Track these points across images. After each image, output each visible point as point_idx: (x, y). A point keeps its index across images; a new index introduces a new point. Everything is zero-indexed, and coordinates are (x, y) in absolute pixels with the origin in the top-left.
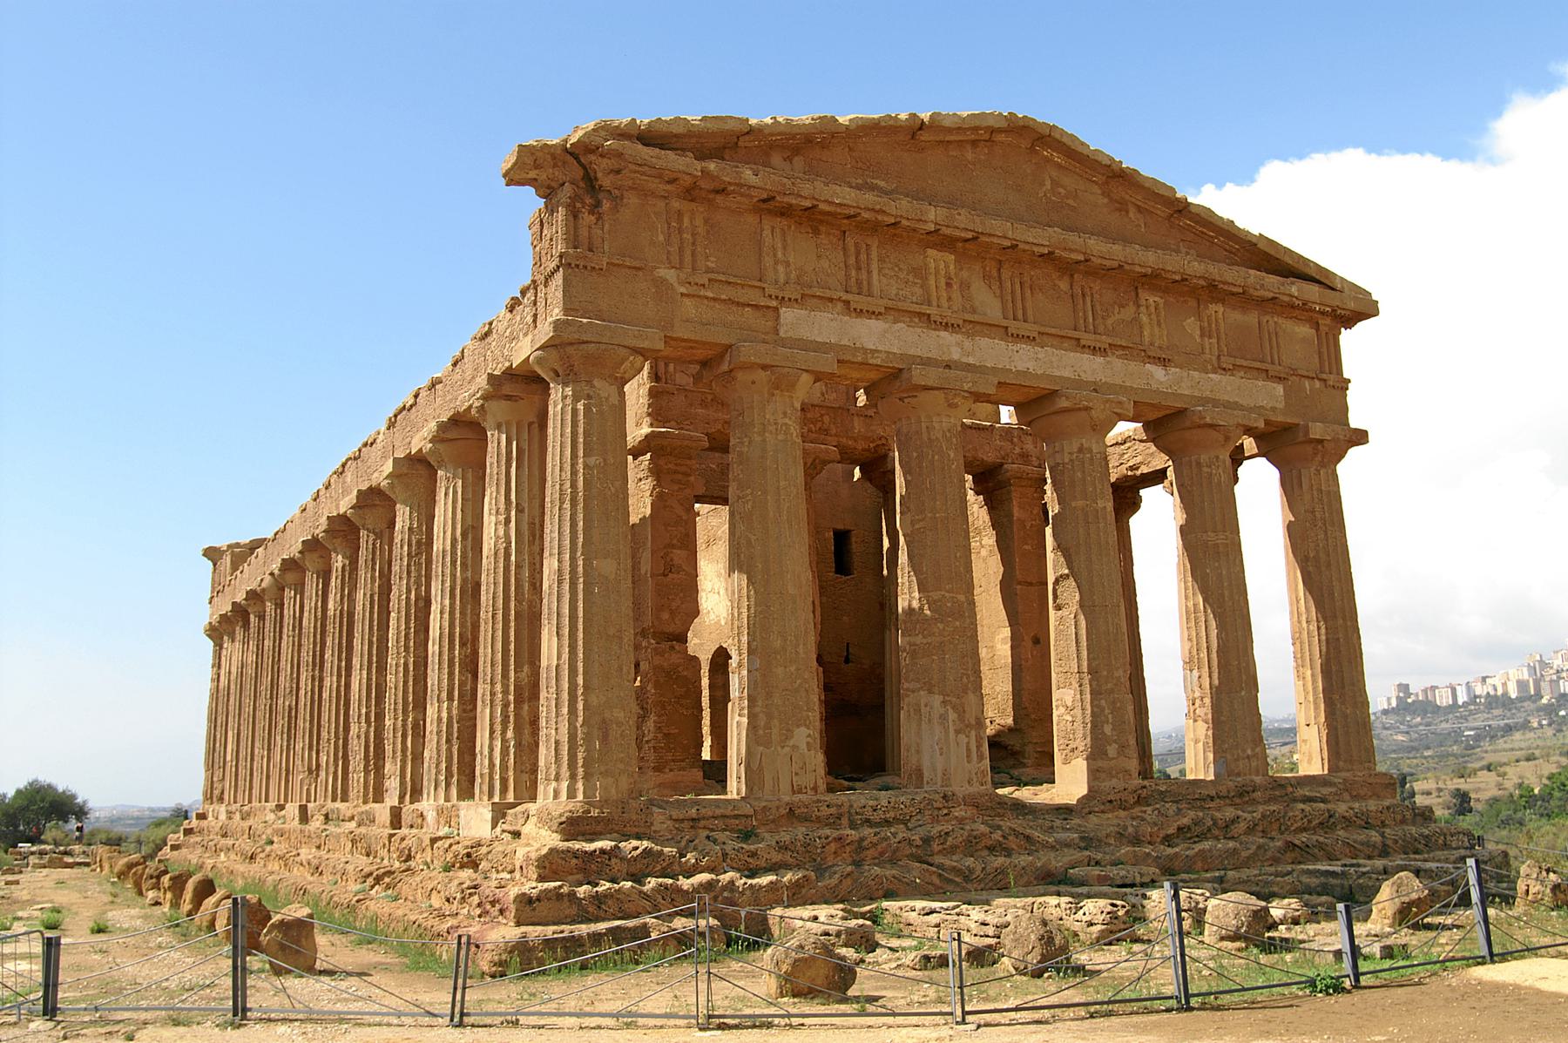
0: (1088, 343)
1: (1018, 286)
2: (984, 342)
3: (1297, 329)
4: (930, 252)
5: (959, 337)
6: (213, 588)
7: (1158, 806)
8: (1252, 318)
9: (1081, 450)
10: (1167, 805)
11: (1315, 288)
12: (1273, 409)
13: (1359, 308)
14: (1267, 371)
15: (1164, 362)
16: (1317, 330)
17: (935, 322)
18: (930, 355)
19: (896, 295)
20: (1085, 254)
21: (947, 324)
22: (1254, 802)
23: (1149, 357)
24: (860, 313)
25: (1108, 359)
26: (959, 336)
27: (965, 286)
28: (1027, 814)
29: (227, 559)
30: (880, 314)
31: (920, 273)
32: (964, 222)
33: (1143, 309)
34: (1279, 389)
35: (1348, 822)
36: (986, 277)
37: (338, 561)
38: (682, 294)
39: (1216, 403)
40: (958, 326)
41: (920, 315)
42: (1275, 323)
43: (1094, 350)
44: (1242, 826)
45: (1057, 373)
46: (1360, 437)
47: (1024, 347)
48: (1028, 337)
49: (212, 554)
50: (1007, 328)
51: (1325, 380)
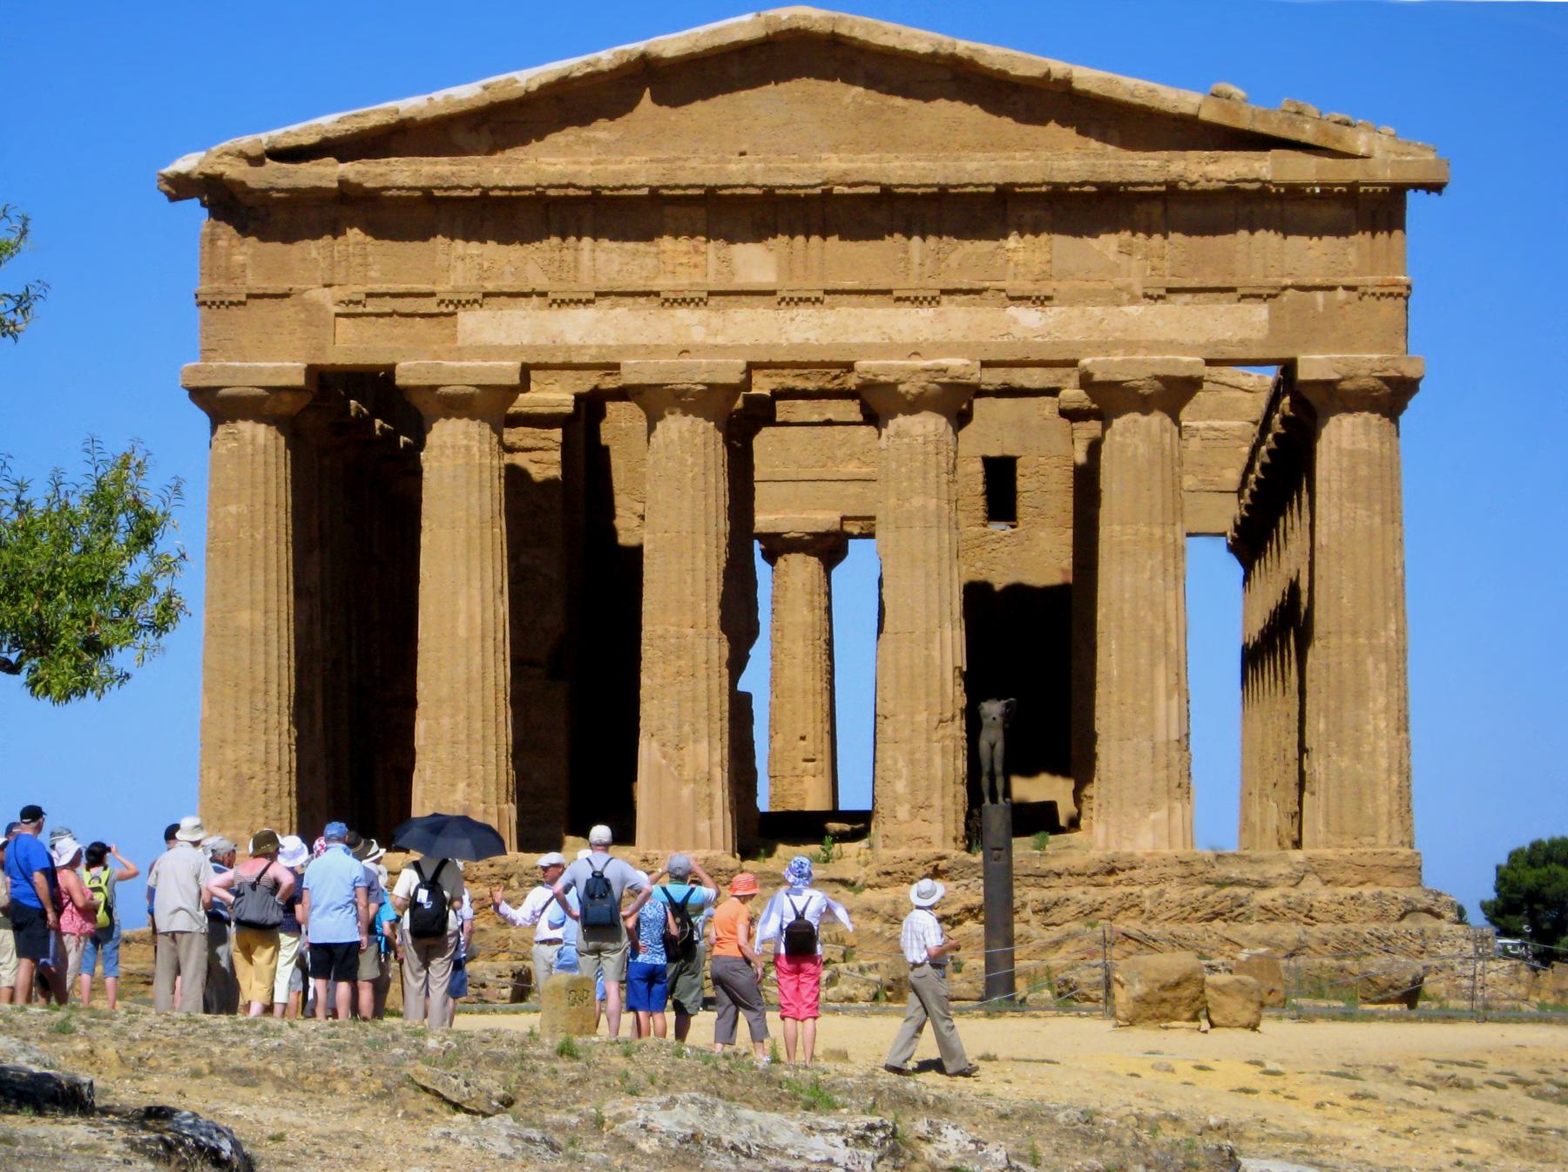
7: (965, 882)
9: (898, 435)
12: (1242, 342)
15: (1043, 301)
17: (667, 300)
19: (620, 271)
22: (1132, 882)
23: (1012, 299)
25: (940, 309)
30: (589, 302)
35: (1270, 914)
38: (338, 315)
39: (1130, 346)
40: (701, 300)
43: (917, 301)
44: (1072, 909)
45: (855, 340)
47: (804, 312)
50: (773, 293)
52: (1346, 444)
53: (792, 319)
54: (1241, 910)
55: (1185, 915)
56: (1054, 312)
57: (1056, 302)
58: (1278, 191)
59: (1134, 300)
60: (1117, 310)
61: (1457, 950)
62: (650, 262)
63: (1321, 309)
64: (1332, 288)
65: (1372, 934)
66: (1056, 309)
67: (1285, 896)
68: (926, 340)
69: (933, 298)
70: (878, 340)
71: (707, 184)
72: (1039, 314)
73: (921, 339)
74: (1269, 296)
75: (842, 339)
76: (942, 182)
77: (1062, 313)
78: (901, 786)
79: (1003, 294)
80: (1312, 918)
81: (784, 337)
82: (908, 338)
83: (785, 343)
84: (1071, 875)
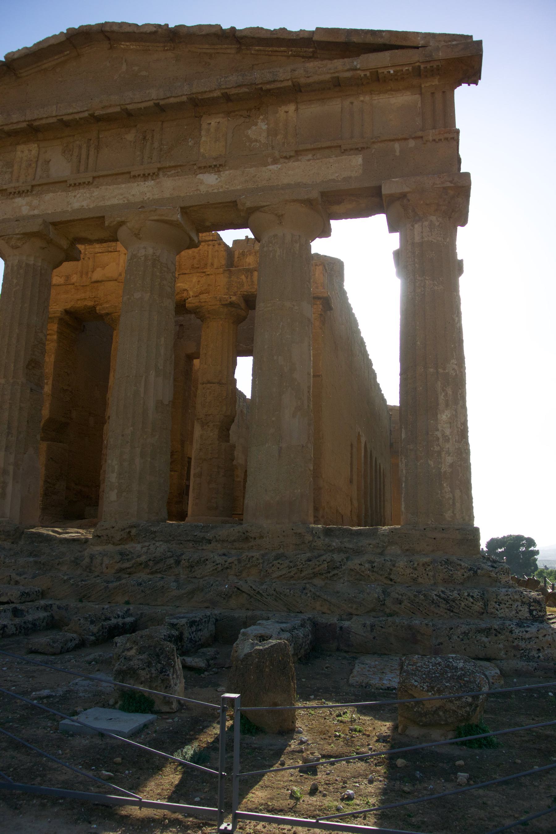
0: (137, 173)
1: (84, 151)
2: (48, 197)
3: (393, 101)
4: (20, 148)
5: (28, 199)
7: (147, 544)
10: (158, 544)
11: (387, 55)
14: (340, 146)
16: (421, 94)
17: (10, 193)
18: (5, 217)
20: (120, 105)
21: (19, 192)
25: (158, 180)
26: (30, 198)
27: (48, 162)
28: (41, 542)
33: (203, 133)
34: (358, 160)
40: (28, 191)
42: (362, 101)
43: (145, 177)
45: (108, 203)
48: (84, 183)
50: (66, 181)
51: (422, 137)
53: (75, 196)
54: (335, 572)
55: (292, 574)
56: (226, 174)
57: (227, 168)
58: (365, 75)
60: (264, 169)
61: (514, 612)
62: (7, 176)
63: (398, 154)
64: (406, 139)
65: (439, 596)
66: (227, 172)
67: (371, 562)
68: (149, 198)
69: (154, 174)
70: (121, 202)
71: (27, 119)
72: (216, 176)
73: (145, 199)
74: (363, 148)
75: (101, 204)
76: (155, 98)
77: (230, 174)
79: (195, 167)
80: (391, 580)
81: (69, 206)
83: (70, 210)
84: (216, 541)
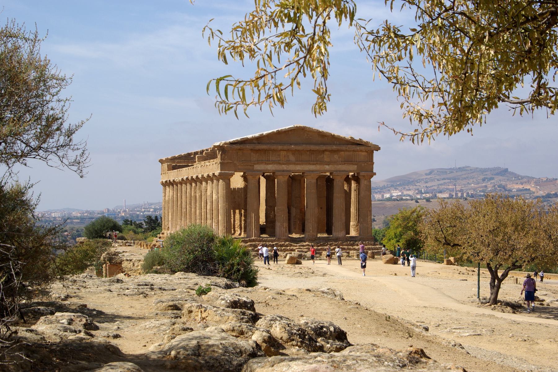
5: (286, 166)
6: (162, 170)
8: (351, 153)
13: (378, 148)
15: (328, 165)
24: (268, 164)
29: (165, 165)
31: (279, 155)
32: (285, 147)
34: (356, 166)
36: (293, 154)
37: (194, 185)
39: (340, 171)
41: (279, 163)
43: (313, 164)
46: (375, 174)
49: (161, 161)
52: (366, 183)
56: (330, 166)
59: (340, 165)
78: (311, 228)
82: (312, 169)
